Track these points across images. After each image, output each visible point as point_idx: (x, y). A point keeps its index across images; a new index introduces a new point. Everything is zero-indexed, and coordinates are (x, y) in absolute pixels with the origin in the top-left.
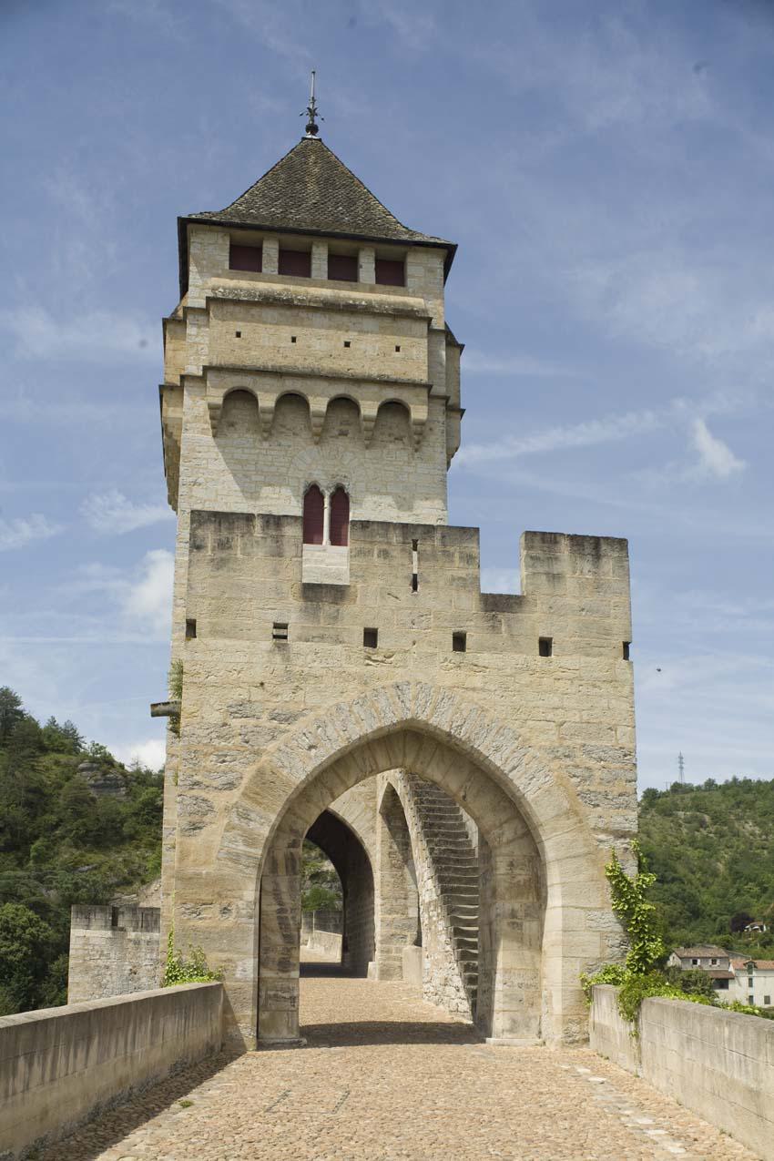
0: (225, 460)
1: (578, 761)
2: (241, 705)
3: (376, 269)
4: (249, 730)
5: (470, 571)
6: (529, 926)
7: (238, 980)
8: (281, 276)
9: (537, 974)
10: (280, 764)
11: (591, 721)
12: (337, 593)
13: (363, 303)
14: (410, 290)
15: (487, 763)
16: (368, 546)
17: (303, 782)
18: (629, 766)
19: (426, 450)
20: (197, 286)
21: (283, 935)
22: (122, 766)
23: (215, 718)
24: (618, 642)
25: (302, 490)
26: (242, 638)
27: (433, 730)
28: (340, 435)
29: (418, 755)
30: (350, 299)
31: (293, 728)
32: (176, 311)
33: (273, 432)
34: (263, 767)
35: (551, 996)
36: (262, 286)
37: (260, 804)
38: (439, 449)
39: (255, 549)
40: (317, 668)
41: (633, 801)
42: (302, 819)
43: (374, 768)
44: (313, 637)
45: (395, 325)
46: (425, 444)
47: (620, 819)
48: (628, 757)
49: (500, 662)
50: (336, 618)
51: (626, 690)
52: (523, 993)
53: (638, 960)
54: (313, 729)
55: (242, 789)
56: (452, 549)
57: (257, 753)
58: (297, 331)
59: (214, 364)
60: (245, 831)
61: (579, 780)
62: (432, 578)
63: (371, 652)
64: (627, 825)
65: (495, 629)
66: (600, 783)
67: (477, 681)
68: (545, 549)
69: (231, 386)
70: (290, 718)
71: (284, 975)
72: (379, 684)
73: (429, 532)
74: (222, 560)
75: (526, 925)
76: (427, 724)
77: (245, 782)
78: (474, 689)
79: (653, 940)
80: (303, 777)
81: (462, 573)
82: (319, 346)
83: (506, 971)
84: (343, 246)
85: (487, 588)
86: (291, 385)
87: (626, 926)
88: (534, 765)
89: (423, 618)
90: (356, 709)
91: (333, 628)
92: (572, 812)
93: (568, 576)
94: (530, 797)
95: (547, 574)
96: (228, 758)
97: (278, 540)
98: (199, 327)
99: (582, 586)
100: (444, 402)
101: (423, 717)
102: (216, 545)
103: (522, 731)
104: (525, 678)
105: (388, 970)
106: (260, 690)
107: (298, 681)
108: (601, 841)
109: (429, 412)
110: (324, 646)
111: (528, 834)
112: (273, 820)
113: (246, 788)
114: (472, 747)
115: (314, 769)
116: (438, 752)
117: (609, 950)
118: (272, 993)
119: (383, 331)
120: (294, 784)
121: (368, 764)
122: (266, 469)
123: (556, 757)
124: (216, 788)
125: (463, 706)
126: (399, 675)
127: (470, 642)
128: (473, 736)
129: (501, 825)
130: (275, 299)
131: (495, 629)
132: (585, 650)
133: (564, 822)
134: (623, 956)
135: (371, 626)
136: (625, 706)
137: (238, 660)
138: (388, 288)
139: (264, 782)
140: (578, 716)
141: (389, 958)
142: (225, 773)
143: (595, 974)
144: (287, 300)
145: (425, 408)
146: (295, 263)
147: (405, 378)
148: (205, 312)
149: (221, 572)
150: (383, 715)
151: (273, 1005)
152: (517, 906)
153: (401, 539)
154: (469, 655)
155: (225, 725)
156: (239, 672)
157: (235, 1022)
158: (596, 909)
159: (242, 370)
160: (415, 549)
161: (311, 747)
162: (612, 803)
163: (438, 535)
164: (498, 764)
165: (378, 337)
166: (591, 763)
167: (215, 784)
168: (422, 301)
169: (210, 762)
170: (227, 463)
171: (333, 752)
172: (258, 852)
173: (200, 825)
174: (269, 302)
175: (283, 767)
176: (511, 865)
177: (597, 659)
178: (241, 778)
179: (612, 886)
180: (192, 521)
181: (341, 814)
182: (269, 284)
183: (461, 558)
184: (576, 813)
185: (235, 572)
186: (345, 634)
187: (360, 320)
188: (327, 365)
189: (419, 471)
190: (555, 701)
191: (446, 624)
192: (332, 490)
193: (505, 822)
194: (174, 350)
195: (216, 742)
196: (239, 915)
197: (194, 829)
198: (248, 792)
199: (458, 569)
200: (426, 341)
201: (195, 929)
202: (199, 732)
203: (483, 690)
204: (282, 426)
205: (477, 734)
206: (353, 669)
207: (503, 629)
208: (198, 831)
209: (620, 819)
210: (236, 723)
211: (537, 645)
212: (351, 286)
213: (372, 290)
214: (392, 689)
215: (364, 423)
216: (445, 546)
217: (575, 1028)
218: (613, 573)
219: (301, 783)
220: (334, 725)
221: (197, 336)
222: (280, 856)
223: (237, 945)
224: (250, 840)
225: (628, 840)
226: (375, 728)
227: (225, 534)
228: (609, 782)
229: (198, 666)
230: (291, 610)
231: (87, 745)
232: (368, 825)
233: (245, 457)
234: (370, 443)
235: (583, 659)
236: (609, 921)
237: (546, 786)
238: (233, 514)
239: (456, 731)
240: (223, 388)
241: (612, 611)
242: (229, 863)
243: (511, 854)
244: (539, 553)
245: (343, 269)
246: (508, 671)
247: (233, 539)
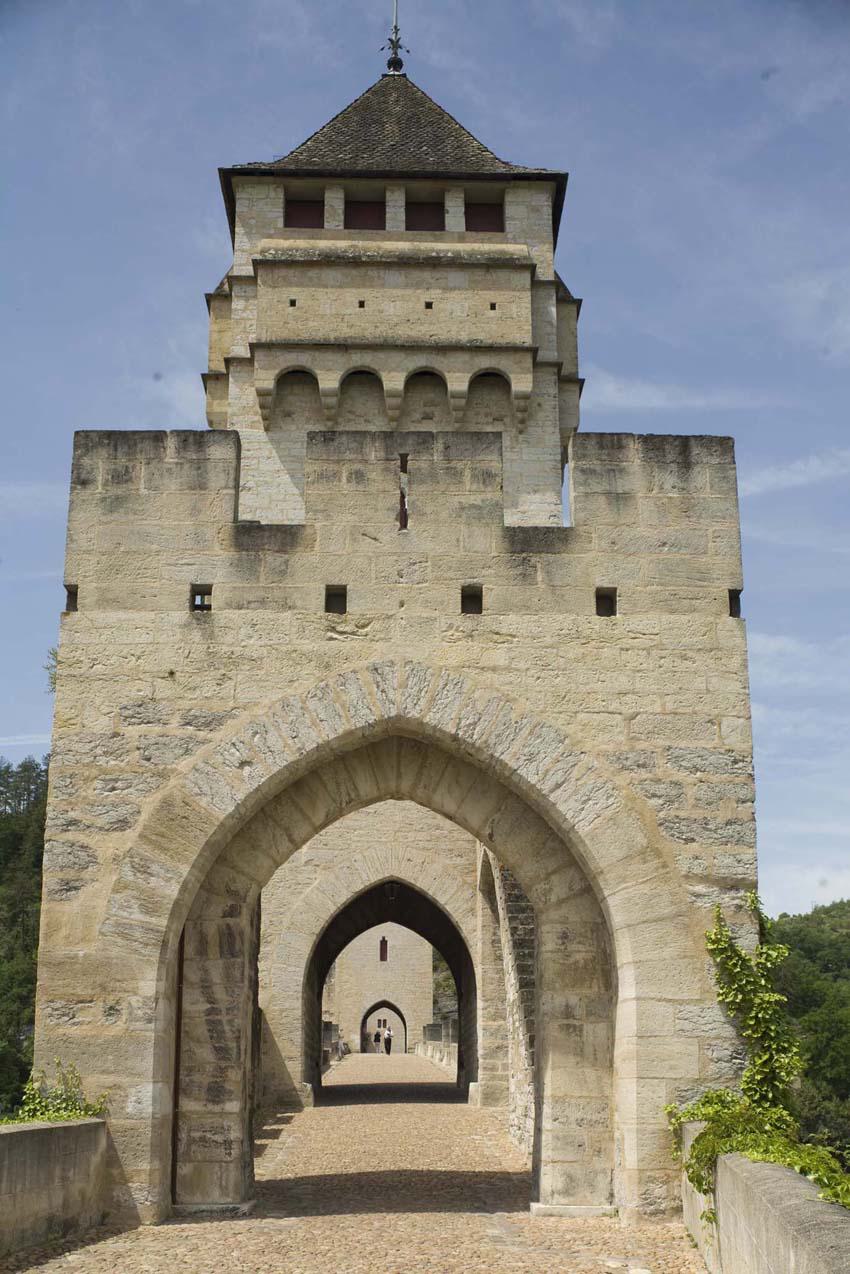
0: (280, 457)
1: (659, 772)
2: (140, 706)
3: (466, 213)
4: (153, 741)
5: (489, 496)
6: (593, 1031)
7: (129, 1117)
8: (346, 231)
9: (606, 1105)
10: (196, 790)
11: (680, 710)
12: (287, 536)
13: (450, 254)
14: (509, 236)
15: (515, 779)
16: (333, 467)
17: (231, 816)
18: (742, 778)
19: (533, 430)
20: (243, 251)
21: (215, 1047)
23: (101, 724)
26: (144, 608)
27: (431, 732)
28: (423, 418)
29: (419, 774)
30: (433, 251)
31: (217, 736)
32: (222, 284)
33: (340, 420)
34: (171, 795)
35: (623, 1139)
36: (324, 244)
37: (164, 850)
38: (550, 429)
39: (166, 481)
40: (254, 646)
41: (748, 832)
42: (243, 873)
43: (353, 796)
44: (249, 602)
45: (489, 277)
46: (532, 423)
47: (729, 861)
48: (741, 764)
49: (534, 626)
50: (283, 573)
51: (735, 663)
52: (584, 1134)
53: (761, 1082)
54: (246, 736)
55: (139, 828)
56: (460, 465)
57: (163, 775)
58: (365, 294)
59: (263, 340)
60: (143, 891)
61: (661, 801)
62: (428, 509)
63: (336, 620)
64: (740, 870)
65: (526, 578)
66: (695, 806)
67: (499, 656)
68: (604, 457)
69: (284, 365)
70: (212, 722)
71: (217, 1108)
72: (347, 667)
73: (424, 442)
74: (117, 498)
75: (588, 1028)
76: (422, 723)
77: (143, 818)
78: (494, 669)
79: (785, 1051)
80: (231, 809)
81: (476, 499)
82: (393, 309)
83: (556, 1100)
85: (512, 519)
86: (358, 360)
87: (740, 1027)
88: (590, 780)
89: (416, 567)
90: (312, 704)
91: (280, 588)
92: (651, 852)
93: (640, 495)
94: (583, 829)
95: (608, 494)
96: (119, 784)
97: (200, 465)
98: (247, 299)
99: (662, 509)
100: (556, 370)
101: (414, 713)
102: (110, 477)
103: (570, 730)
104: (574, 650)
105: (493, 1093)
106: (168, 683)
107: (222, 665)
108: (698, 896)
109: (535, 382)
111: (588, 891)
112: (185, 874)
113: (145, 827)
114: (492, 756)
115: (248, 796)
116: (450, 768)
117: (713, 1067)
118: (196, 1135)
119: (473, 286)
120: (218, 819)
121: (343, 789)
123: (624, 768)
124: (101, 829)
125: (476, 695)
126: (378, 652)
128: (492, 741)
129: (548, 875)
130: (338, 257)
131: (526, 578)
132: (669, 605)
133: (636, 867)
134: (737, 1076)
135: (336, 581)
136: (736, 686)
137: (137, 640)
138: (481, 235)
139: (172, 817)
140: (659, 703)
141: (493, 1078)
142: (115, 805)
143: (689, 1105)
144: (353, 258)
145: (530, 377)
146: (365, 214)
147: (503, 341)
148: (252, 280)
149: (116, 515)
150: (352, 712)
151: (198, 1152)
152: (573, 1000)
153: (382, 454)
154: (487, 619)
155: (115, 735)
156: (139, 658)
157: (125, 1180)
158: (689, 1002)
159: (297, 344)
160: (404, 469)
161: (243, 764)
162: (716, 836)
163: (439, 445)
164: (533, 780)
165: (469, 293)
167: (100, 822)
168: (524, 247)
169: (93, 791)
170: (282, 462)
171: (276, 769)
172: (162, 922)
173: (77, 884)
174: (329, 261)
175: (202, 794)
176: (564, 936)
177: (687, 617)
178: (139, 812)
179: (717, 965)
180: (76, 447)
181: (430, 893)
182: (334, 239)
183: (474, 476)
184: (658, 854)
185: (135, 514)
186: (296, 595)
187: (445, 274)
188: (405, 333)
189: (525, 457)
190: (622, 682)
191: (451, 574)
193: (554, 872)
194: (220, 332)
195: (102, 761)
196: (132, 1018)
197: (68, 890)
198: (147, 833)
199: (470, 493)
200: (529, 294)
201: (67, 1040)
202: (76, 747)
203: (508, 669)
204: (349, 412)
205: (498, 736)
206: (307, 645)
207: (539, 579)
208: (74, 892)
209: (729, 861)
210: (132, 732)
211: (593, 601)
212: (435, 235)
213: (461, 239)
214: (367, 673)
215: (452, 401)
216: (449, 461)
217: (659, 1191)
218: (712, 487)
219: (226, 818)
220: (278, 728)
221: (244, 311)
222: (211, 930)
223: (129, 1063)
224: (149, 906)
225: (742, 893)
226: (341, 731)
227: (123, 461)
228: (709, 804)
229: (80, 651)
230: (218, 566)
232: (465, 906)
235: (666, 617)
236: (714, 1021)
237: (608, 813)
238: (135, 433)
239: (466, 732)
240: (275, 368)
241: (711, 544)
242: (119, 940)
243: (564, 921)
244: (596, 465)
245: (425, 216)
246: (548, 640)
247: (134, 467)
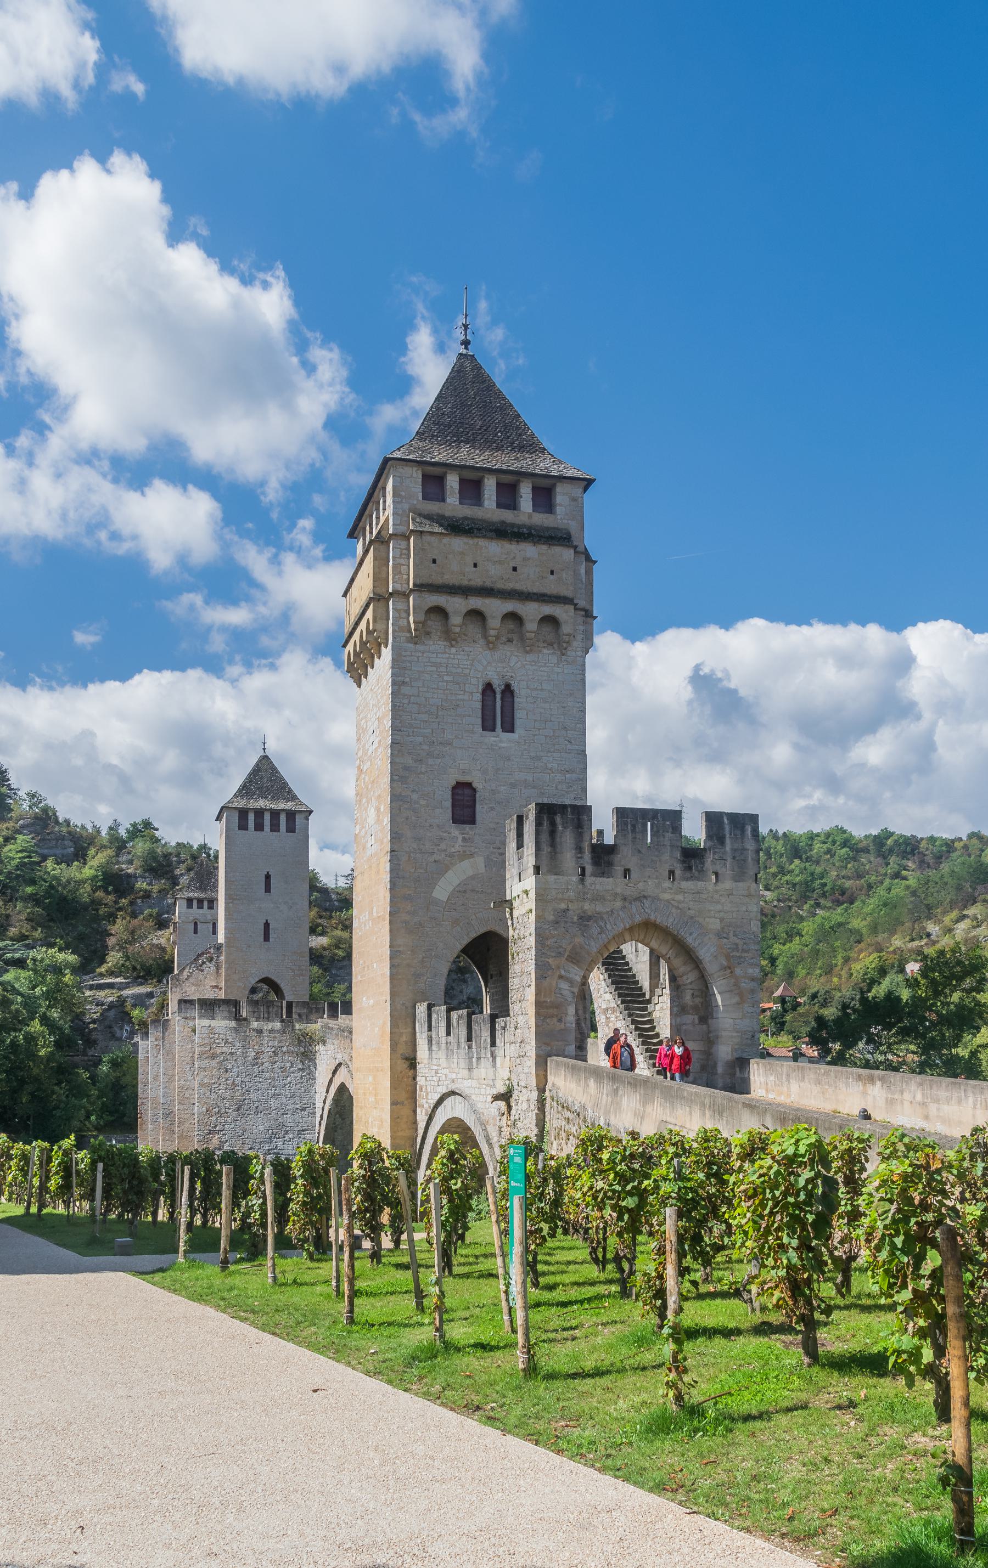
12: (611, 849)
25: (480, 688)
38: (580, 653)
84: (507, 479)
90: (621, 913)
122: (454, 670)
127: (678, 873)
166: (738, 941)
172: (576, 990)
192: (503, 687)
206: (619, 890)
233: (438, 660)
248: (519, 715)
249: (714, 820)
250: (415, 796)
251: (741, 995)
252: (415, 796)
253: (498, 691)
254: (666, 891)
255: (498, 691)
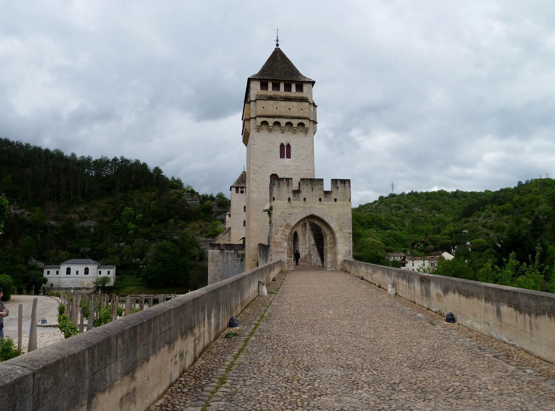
19: (308, 134)
22: (198, 193)
23: (279, 214)
24: (349, 198)
65: (326, 197)
70: (291, 214)
82: (283, 108)
97: (288, 182)
110: (297, 201)
169: (278, 222)
172: (287, 238)
199: (320, 187)
224: (285, 235)
230: (291, 195)
231: (185, 186)
234: (295, 132)
248: (292, 153)
249: (334, 182)
250: (258, 179)
251: (345, 238)
252: (258, 179)
253: (285, 146)
254: (317, 205)
255: (285, 146)
